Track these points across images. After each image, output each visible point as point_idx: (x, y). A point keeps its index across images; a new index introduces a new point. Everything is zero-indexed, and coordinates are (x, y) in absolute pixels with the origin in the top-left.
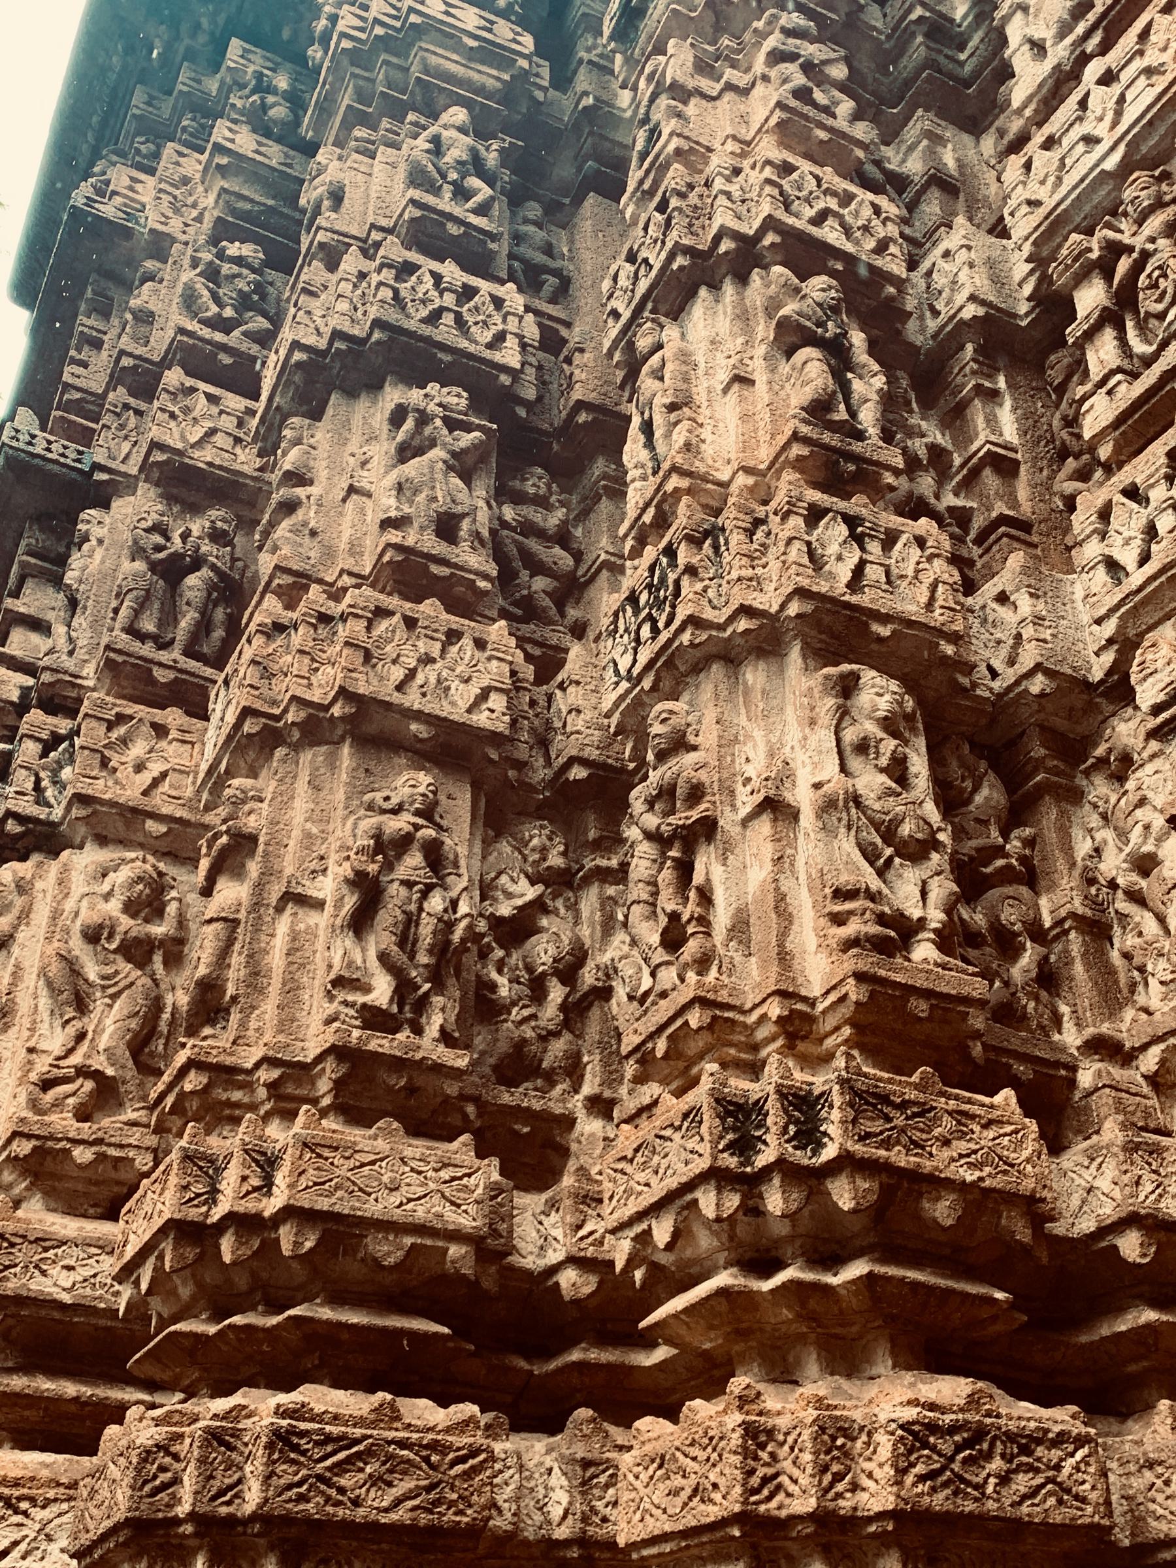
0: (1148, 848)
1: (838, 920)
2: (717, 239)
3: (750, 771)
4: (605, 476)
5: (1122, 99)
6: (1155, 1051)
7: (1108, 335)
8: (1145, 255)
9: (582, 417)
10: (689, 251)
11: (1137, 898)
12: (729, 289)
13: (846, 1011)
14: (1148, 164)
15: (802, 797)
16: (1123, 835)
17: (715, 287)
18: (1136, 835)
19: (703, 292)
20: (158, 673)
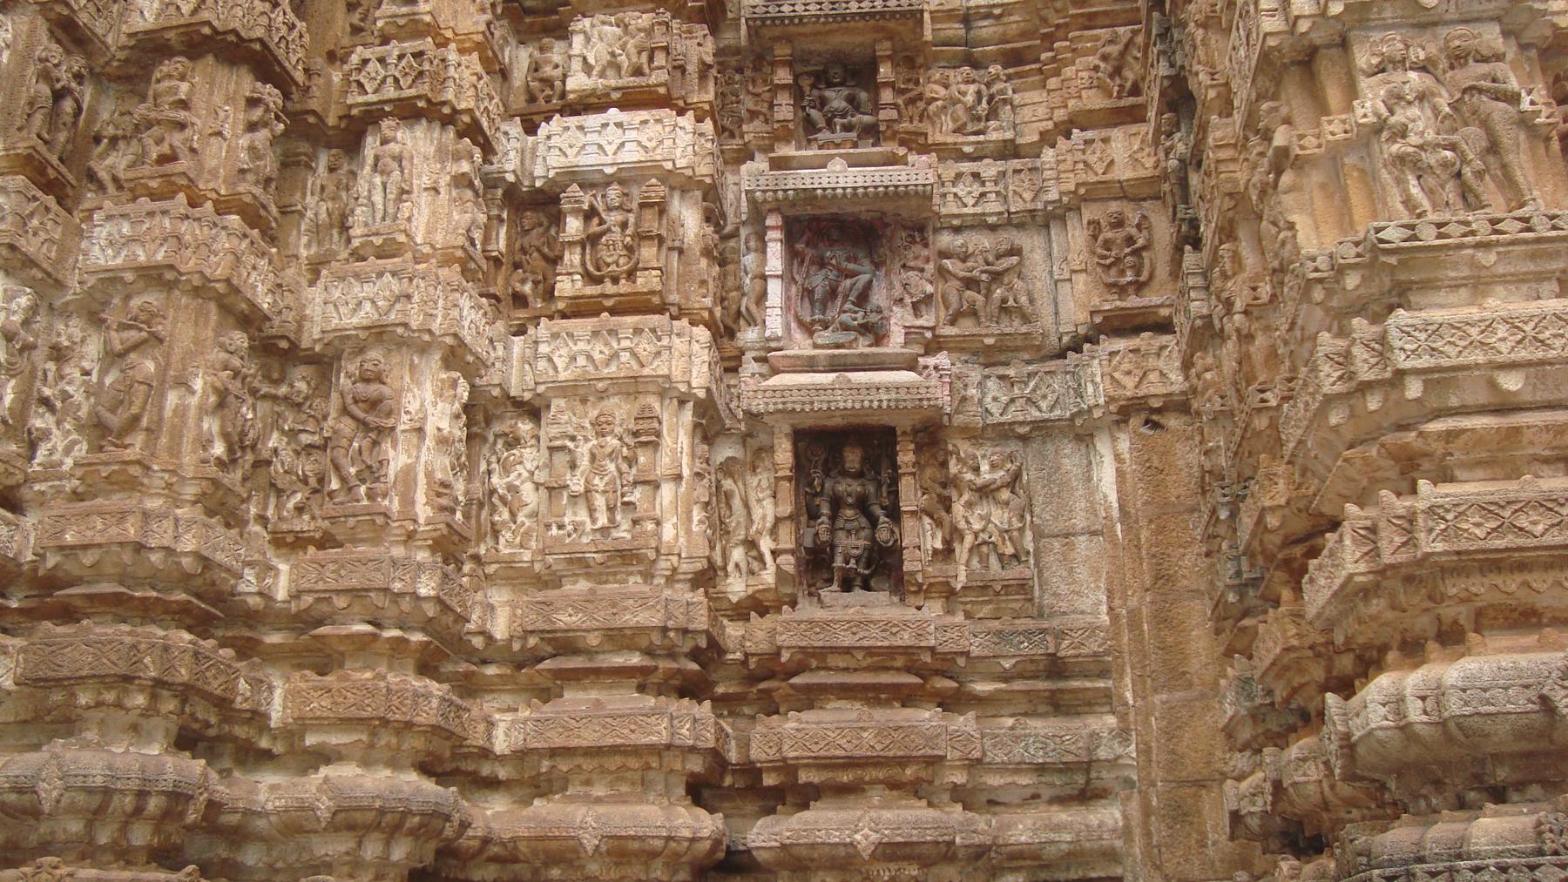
0: (517, 483)
1: (439, 495)
2: (444, 103)
3: (411, 408)
4: (305, 154)
5: (623, 144)
6: (495, 566)
7: (578, 250)
8: (609, 230)
9: (311, 120)
10: (429, 101)
11: (505, 503)
12: (437, 126)
13: (434, 534)
14: (622, 182)
15: (430, 429)
16: (506, 470)
17: (430, 121)
18: (513, 476)
19: (424, 122)
20: (50, 171)
